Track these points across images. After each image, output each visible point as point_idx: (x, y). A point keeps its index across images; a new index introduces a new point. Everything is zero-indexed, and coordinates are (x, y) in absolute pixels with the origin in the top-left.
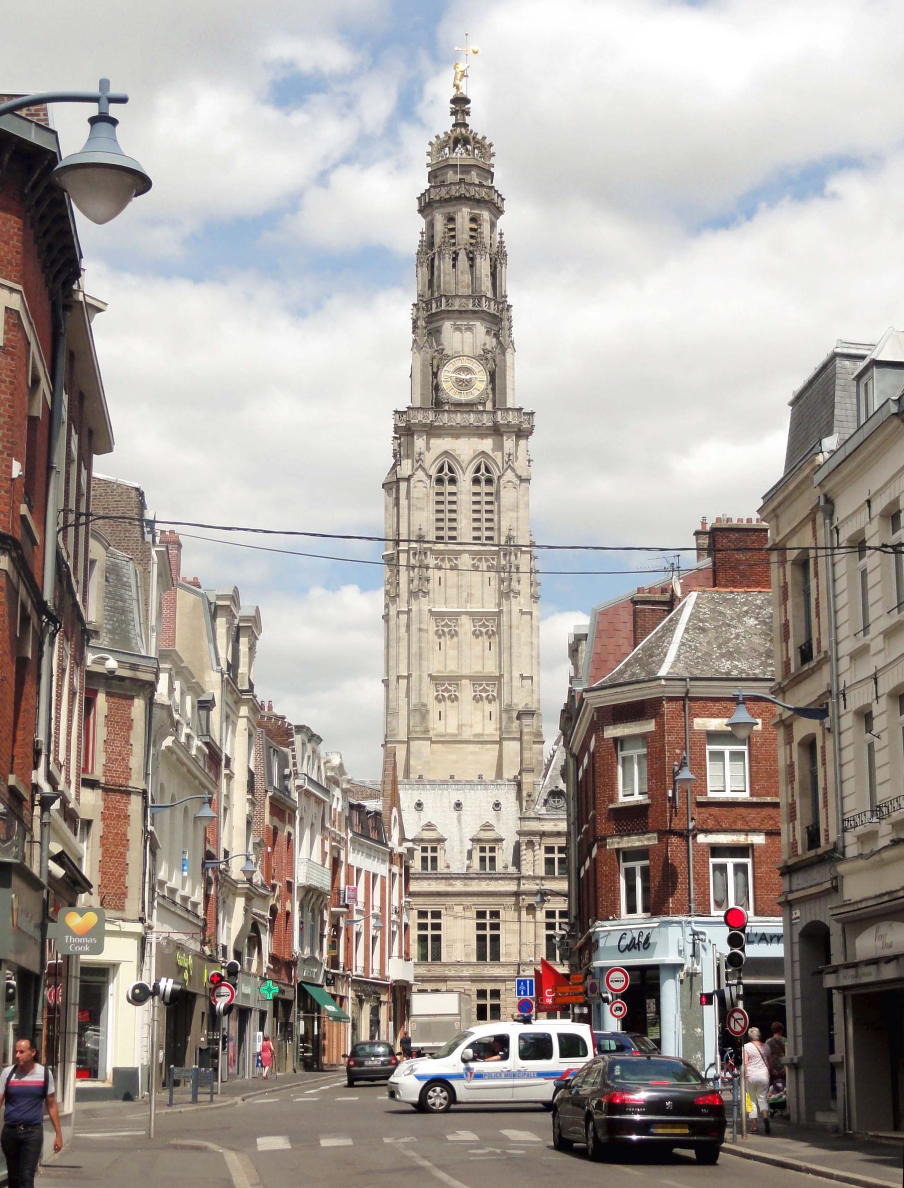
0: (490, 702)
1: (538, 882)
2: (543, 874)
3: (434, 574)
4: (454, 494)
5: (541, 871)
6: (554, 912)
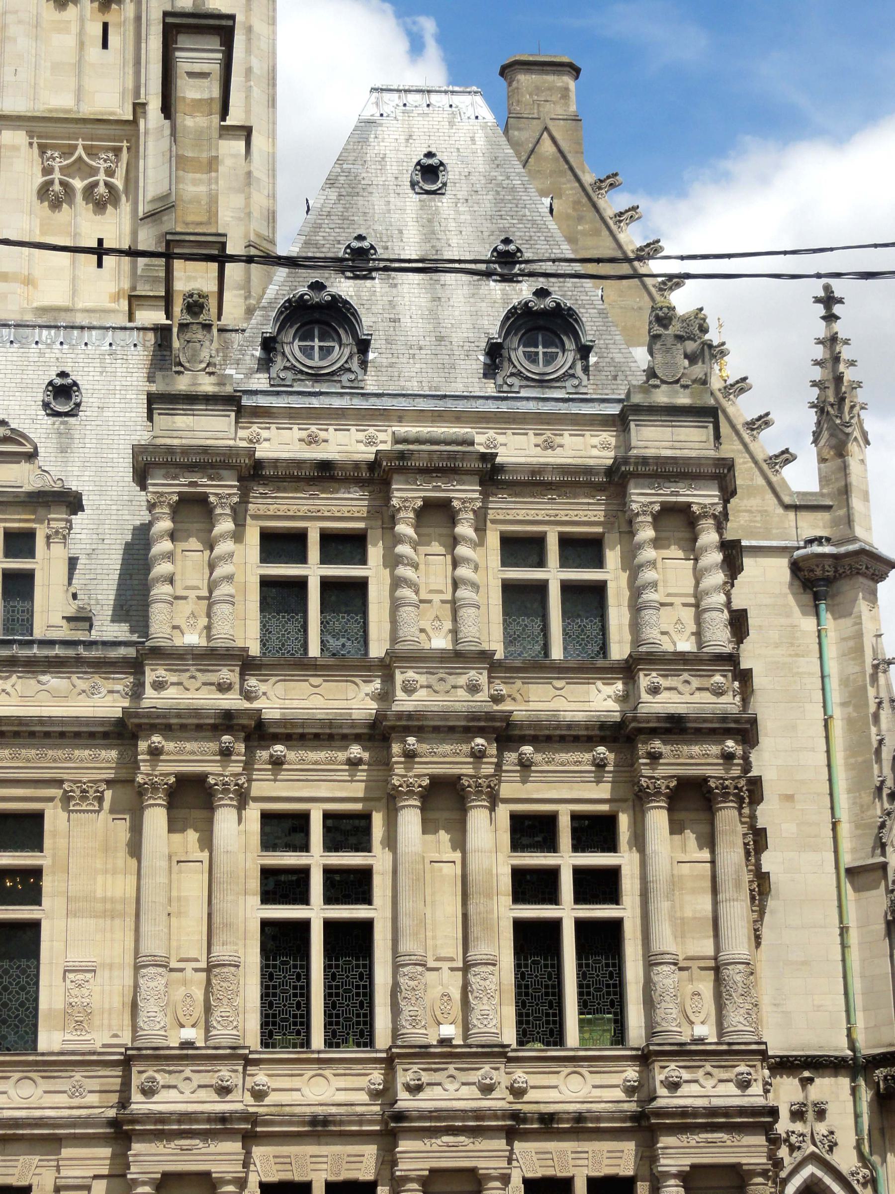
0: (100, 206)
1: (228, 674)
2: (250, 638)
5: (244, 627)
6: (304, 818)
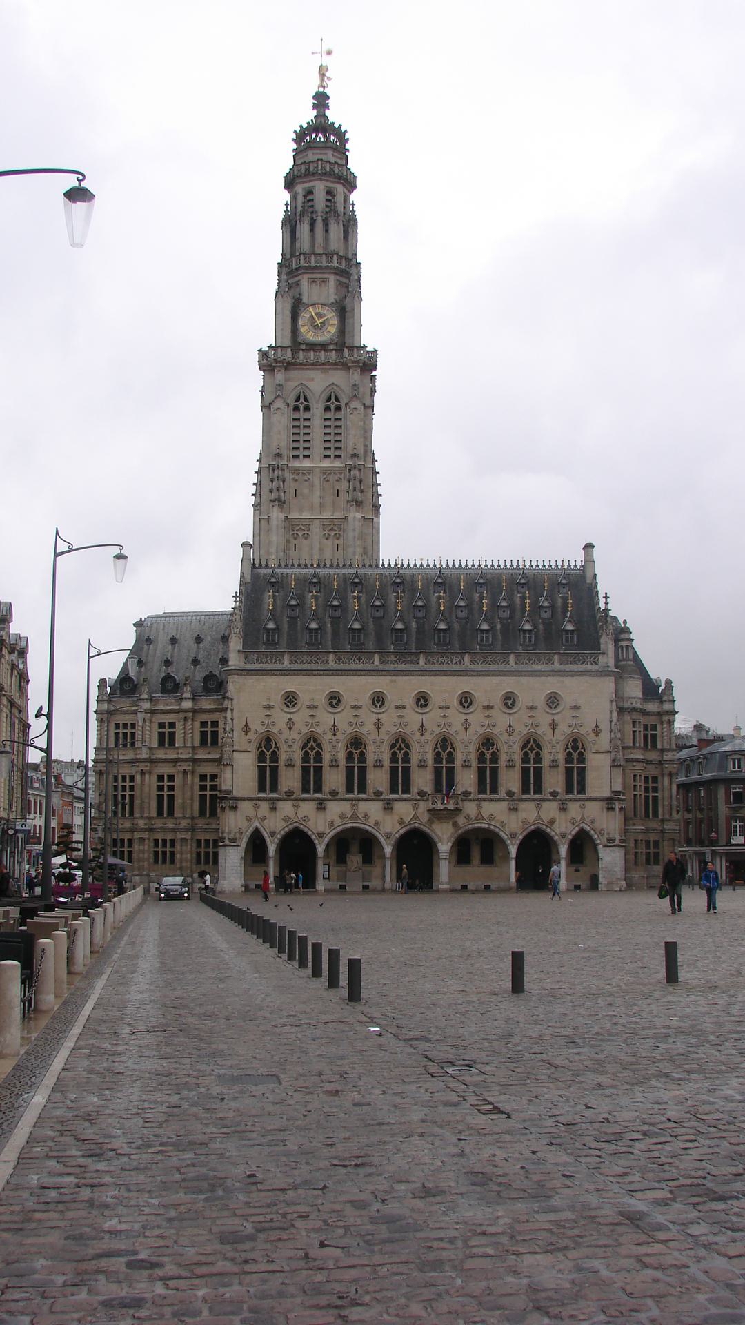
3: (290, 487)
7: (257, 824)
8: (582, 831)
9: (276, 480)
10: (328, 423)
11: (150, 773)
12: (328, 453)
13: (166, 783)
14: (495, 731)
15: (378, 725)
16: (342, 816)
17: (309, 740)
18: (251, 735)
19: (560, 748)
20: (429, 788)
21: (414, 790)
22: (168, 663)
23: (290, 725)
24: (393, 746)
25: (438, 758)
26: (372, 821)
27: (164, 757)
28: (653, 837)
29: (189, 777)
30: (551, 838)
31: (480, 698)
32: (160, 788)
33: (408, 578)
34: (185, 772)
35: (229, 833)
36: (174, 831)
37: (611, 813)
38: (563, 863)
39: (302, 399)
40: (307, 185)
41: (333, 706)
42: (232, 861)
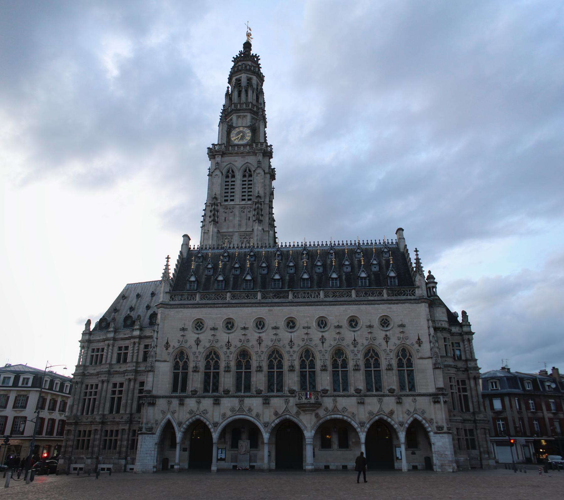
4: (234, 181)
7: (169, 416)
8: (415, 421)
9: (214, 211)
10: (244, 183)
11: (108, 382)
12: (244, 198)
13: (118, 389)
14: (344, 343)
15: (260, 341)
16: (233, 410)
17: (211, 353)
18: (171, 350)
19: (392, 355)
20: (296, 387)
21: (286, 389)
22: (132, 309)
23: (198, 342)
24: (270, 356)
25: (303, 365)
26: (254, 413)
27: (118, 370)
28: (469, 426)
29: (132, 383)
30: (392, 426)
31: (332, 320)
32: (114, 392)
33: (285, 253)
34: (130, 380)
35: (147, 424)
36: (118, 423)
37: (437, 406)
38: (403, 448)
39: (230, 171)
40: (237, 77)
41: (229, 329)
42: (147, 445)
